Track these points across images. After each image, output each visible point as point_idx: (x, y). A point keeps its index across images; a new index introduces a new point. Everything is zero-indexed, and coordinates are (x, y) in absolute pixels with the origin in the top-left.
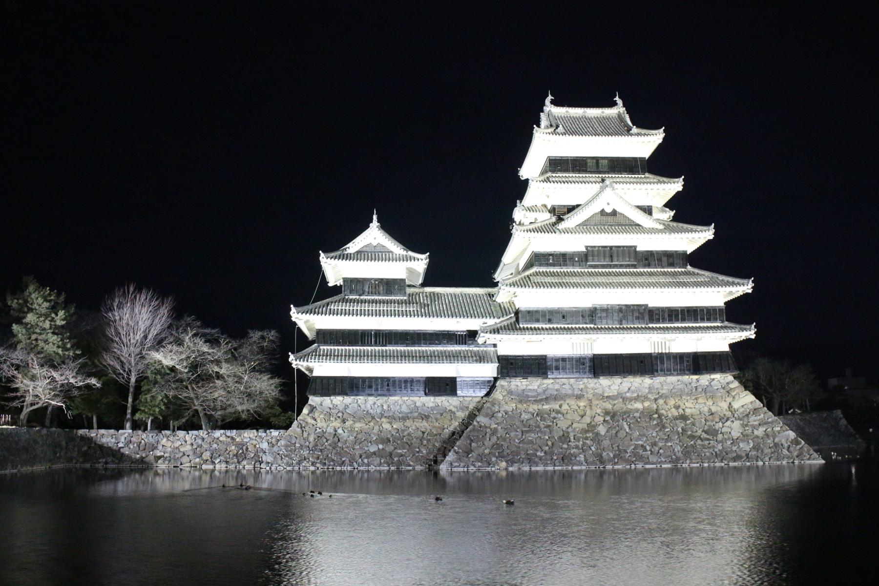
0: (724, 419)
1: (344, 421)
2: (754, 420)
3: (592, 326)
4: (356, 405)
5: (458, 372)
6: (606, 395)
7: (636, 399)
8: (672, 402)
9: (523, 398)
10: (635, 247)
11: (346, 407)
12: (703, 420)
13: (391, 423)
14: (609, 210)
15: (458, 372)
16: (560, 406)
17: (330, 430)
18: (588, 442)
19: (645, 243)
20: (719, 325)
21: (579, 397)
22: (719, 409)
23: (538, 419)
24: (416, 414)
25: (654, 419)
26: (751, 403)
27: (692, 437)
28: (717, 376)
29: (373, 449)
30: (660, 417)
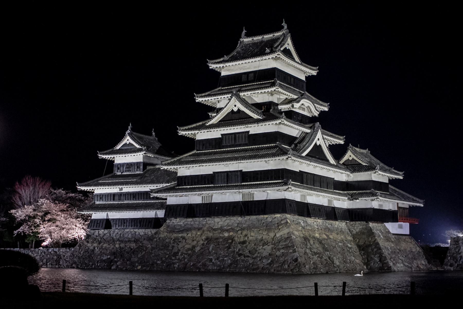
4: (108, 234)
6: (214, 228)
7: (228, 231)
8: (244, 233)
9: (173, 230)
11: (105, 235)
13: (120, 244)
14: (235, 109)
17: (92, 248)
18: (186, 256)
19: (254, 129)
20: (280, 181)
21: (199, 229)
24: (133, 239)
28: (278, 215)
29: (105, 258)
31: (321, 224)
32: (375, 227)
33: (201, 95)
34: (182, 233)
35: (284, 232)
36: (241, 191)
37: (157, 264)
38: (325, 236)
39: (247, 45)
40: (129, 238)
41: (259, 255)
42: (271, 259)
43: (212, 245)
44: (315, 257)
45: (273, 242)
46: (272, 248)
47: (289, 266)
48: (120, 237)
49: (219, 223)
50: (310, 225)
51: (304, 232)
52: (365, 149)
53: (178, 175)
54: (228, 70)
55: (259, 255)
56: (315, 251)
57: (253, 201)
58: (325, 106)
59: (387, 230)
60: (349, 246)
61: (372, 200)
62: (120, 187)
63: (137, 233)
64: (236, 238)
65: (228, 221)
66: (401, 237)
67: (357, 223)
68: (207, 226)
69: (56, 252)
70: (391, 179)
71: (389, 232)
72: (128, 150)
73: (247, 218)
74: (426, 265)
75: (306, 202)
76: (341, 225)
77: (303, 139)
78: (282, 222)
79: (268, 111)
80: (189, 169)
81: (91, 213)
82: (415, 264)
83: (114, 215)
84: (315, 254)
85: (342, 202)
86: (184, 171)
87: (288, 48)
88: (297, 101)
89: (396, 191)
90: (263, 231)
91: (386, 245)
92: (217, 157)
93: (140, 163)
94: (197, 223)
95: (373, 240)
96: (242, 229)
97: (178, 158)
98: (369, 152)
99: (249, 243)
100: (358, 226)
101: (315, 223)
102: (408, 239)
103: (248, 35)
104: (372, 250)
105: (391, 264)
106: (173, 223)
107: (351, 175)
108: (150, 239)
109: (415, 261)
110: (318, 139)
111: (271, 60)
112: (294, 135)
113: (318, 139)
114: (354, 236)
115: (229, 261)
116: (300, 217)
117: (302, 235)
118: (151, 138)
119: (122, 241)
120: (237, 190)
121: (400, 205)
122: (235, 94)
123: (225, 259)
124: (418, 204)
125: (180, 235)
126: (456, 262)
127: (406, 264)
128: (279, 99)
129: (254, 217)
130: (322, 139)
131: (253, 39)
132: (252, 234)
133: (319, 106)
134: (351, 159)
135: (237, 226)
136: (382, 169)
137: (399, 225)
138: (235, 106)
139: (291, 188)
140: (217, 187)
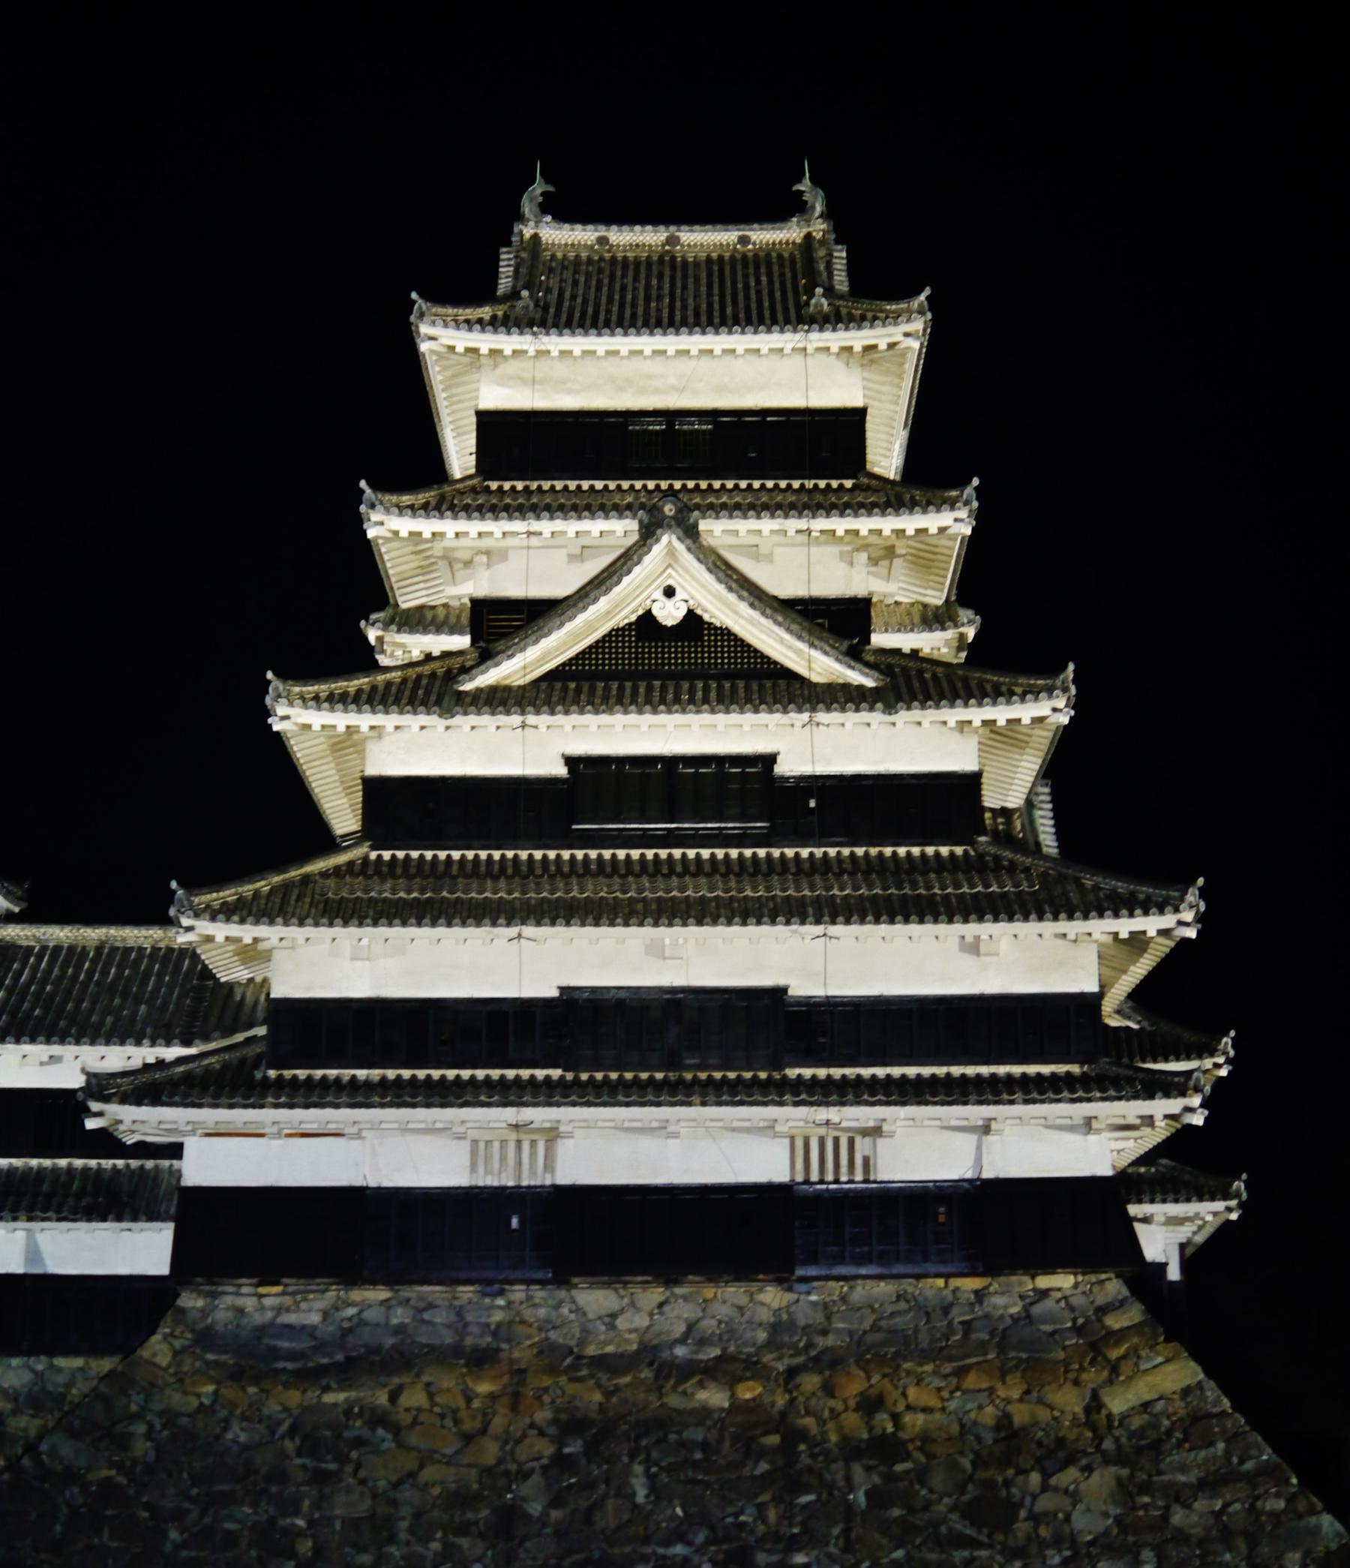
0: (1058, 1454)
2: (1185, 1465)
3: (556, 1073)
5: (33, 1253)
6: (591, 1350)
8: (854, 1385)
9: (254, 1357)
10: (770, 759)
12: (966, 1463)
14: (670, 614)
15: (33, 1253)
16: (394, 1397)
18: (464, 1542)
19: (811, 747)
20: (1075, 1069)
21: (480, 1360)
22: (1044, 1415)
23: (289, 1445)
25: (763, 1453)
26: (1186, 1392)
27: (903, 1532)
28: (1063, 1281)
30: (788, 1449)
34: (344, 1385)
45: (1108, 1444)
49: (621, 1323)
55: (1044, 1532)
92: (653, 891)
106: (240, 1311)
108: (97, 1421)
111: (838, 365)
131: (603, 241)
135: (770, 1344)
138: (669, 592)
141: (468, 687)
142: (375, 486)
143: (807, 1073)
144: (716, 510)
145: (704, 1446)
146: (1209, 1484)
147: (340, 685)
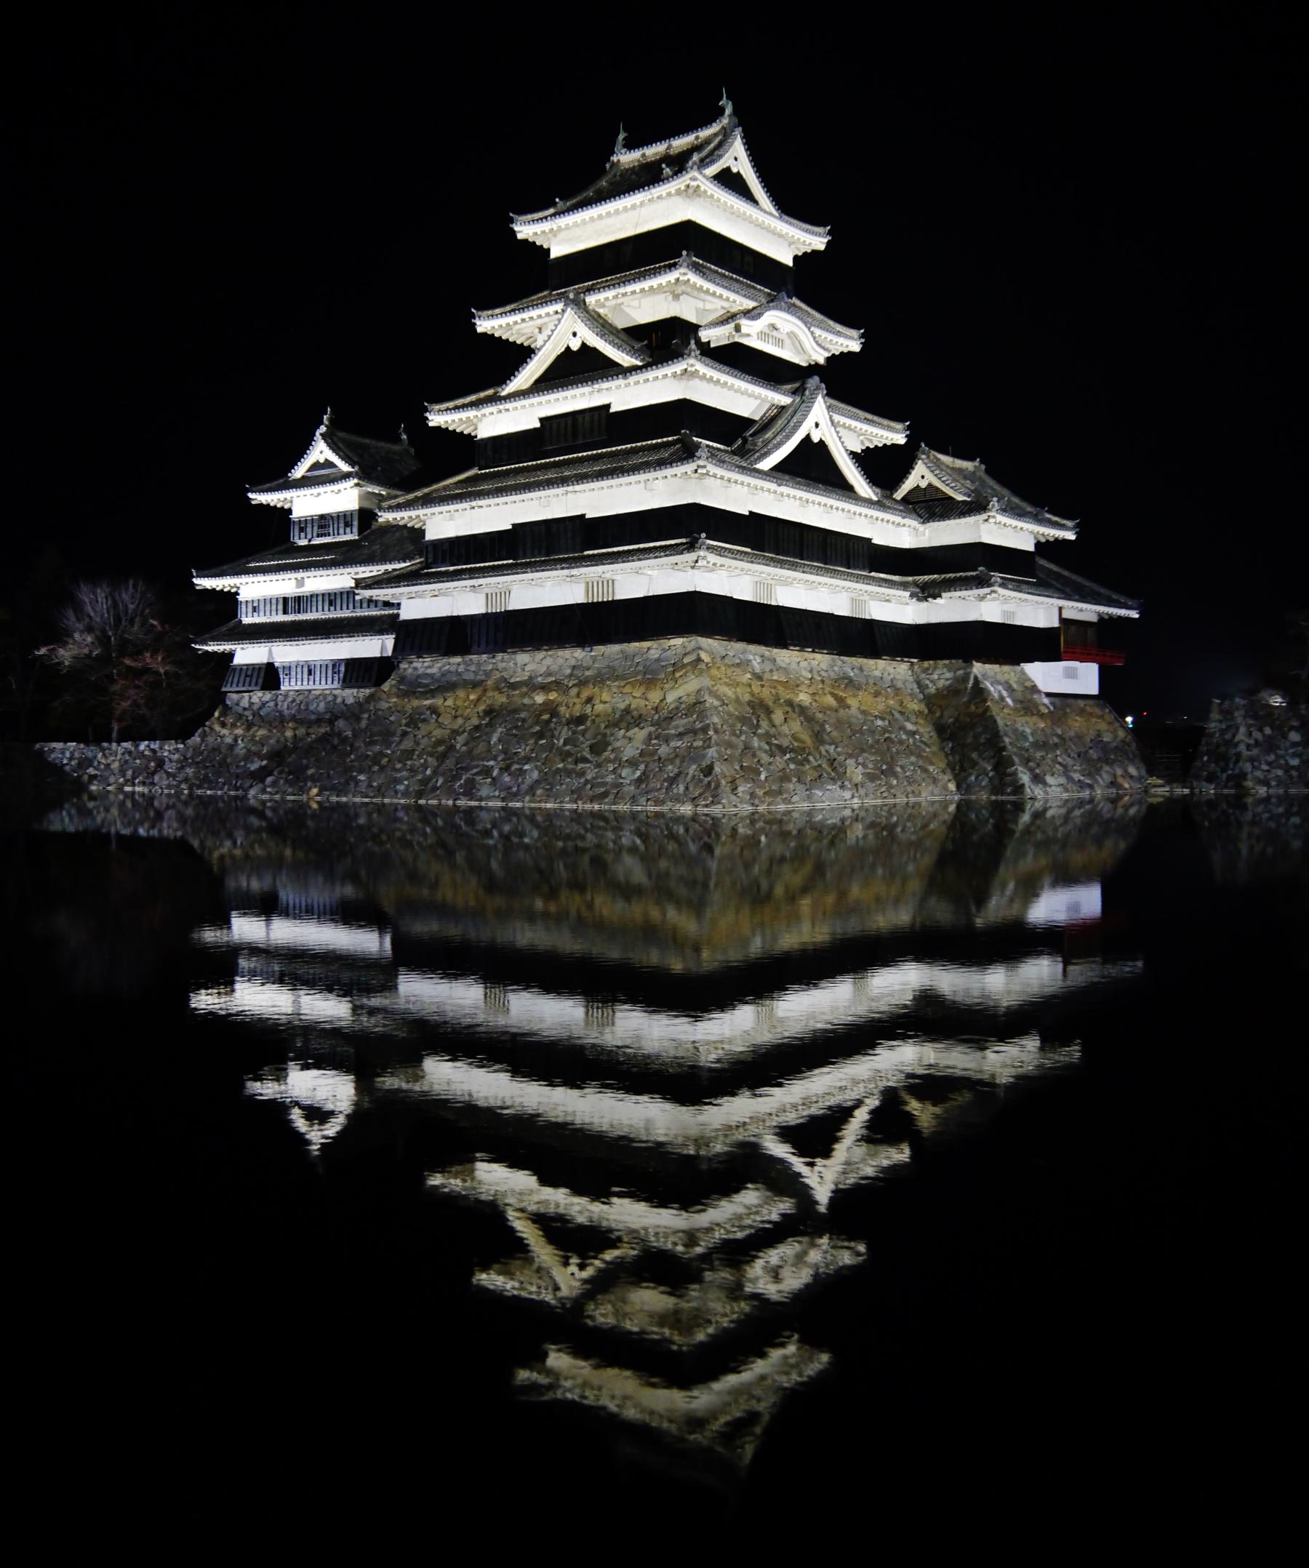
1: (249, 726)
4: (272, 704)
7: (545, 688)
8: (585, 695)
9: (413, 688)
10: (608, 406)
11: (264, 704)
13: (294, 729)
14: (575, 346)
17: (229, 740)
19: (623, 395)
20: (684, 540)
21: (475, 685)
28: (677, 642)
31: (824, 666)
32: (990, 673)
33: (490, 312)
34: (433, 697)
35: (686, 688)
36: (575, 572)
37: (357, 782)
38: (830, 700)
39: (627, 170)
40: (319, 714)
41: (612, 757)
42: (642, 767)
43: (500, 730)
44: (779, 761)
46: (650, 734)
47: (687, 788)
48: (299, 710)
49: (527, 668)
50: (786, 671)
51: (756, 689)
52: (972, 459)
53: (430, 535)
54: (568, 241)
56: (785, 742)
57: (613, 601)
58: (851, 338)
59: (1028, 684)
60: (910, 726)
61: (982, 598)
62: (300, 574)
63: (339, 700)
64: (562, 709)
65: (548, 661)
66: (1071, 701)
67: (941, 663)
68: (497, 675)
69: (154, 751)
70: (1043, 540)
71: (1034, 689)
72: (321, 477)
73: (599, 650)
74: (1140, 779)
75: (773, 603)
76: (896, 670)
77: (768, 423)
78: (686, 661)
79: (663, 341)
80: (451, 519)
81: (233, 647)
82: (1105, 776)
83: (283, 653)
84: (783, 750)
85: (894, 606)
86: (445, 522)
87: (735, 170)
88: (750, 314)
89: (1058, 576)
90: (634, 687)
91: (1018, 726)
93: (352, 513)
94: (473, 668)
95: (980, 710)
96: (582, 683)
97: (426, 490)
98: (983, 467)
99: (594, 721)
100: (941, 675)
101: (804, 664)
102: (1091, 707)
103: (630, 145)
104: (976, 737)
105: (1025, 778)
106: (416, 669)
107: (921, 528)
109: (1107, 768)
110: (817, 425)
111: (678, 200)
112: (745, 413)
113: (817, 425)
114: (930, 701)
115: (535, 775)
116: (752, 648)
117: (747, 697)
118: (396, 448)
119: (300, 722)
120: (566, 572)
121: (1066, 615)
122: (573, 301)
123: (526, 767)
124: (1122, 612)
125: (427, 702)
126: (1223, 770)
127: (1077, 776)
128: (699, 312)
129: (614, 649)
130: (844, 432)
131: (643, 155)
132: (605, 696)
133: (830, 337)
134: (923, 484)
135: (571, 675)
136: (1009, 510)
137: (1066, 669)
138: (575, 334)
139: (704, 558)
140: (521, 564)
141: (503, 394)
142: (477, 309)
143: (591, 552)
144: (590, 290)
145: (524, 720)
146: (680, 735)
147: (460, 402)
